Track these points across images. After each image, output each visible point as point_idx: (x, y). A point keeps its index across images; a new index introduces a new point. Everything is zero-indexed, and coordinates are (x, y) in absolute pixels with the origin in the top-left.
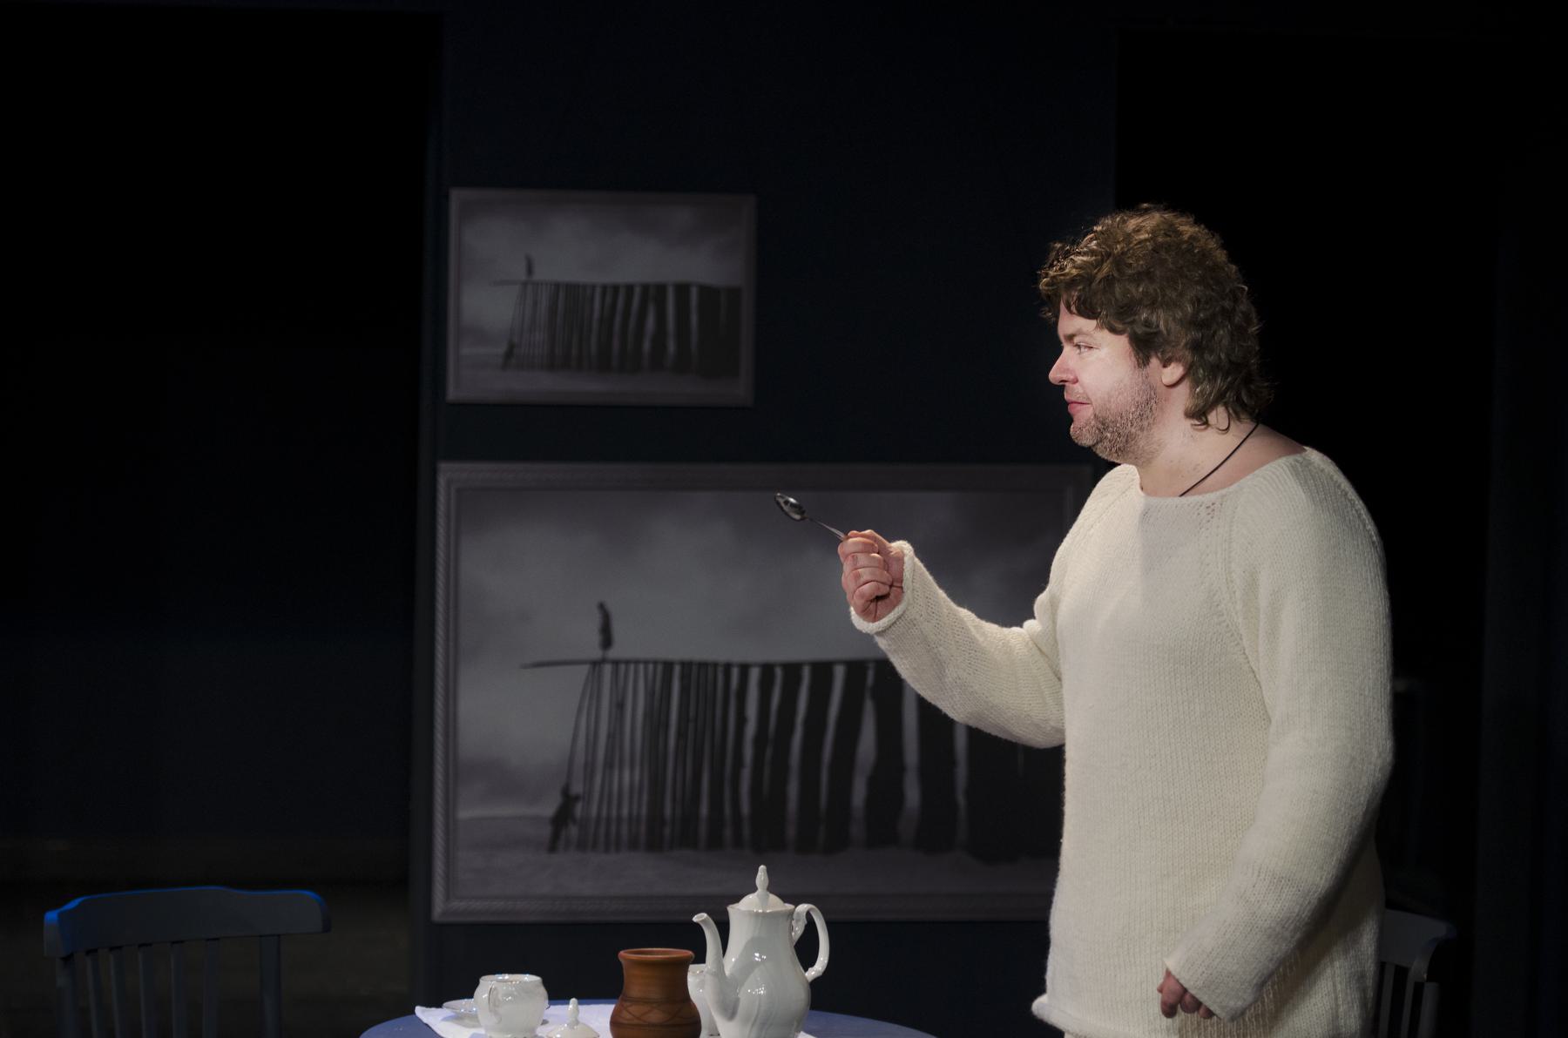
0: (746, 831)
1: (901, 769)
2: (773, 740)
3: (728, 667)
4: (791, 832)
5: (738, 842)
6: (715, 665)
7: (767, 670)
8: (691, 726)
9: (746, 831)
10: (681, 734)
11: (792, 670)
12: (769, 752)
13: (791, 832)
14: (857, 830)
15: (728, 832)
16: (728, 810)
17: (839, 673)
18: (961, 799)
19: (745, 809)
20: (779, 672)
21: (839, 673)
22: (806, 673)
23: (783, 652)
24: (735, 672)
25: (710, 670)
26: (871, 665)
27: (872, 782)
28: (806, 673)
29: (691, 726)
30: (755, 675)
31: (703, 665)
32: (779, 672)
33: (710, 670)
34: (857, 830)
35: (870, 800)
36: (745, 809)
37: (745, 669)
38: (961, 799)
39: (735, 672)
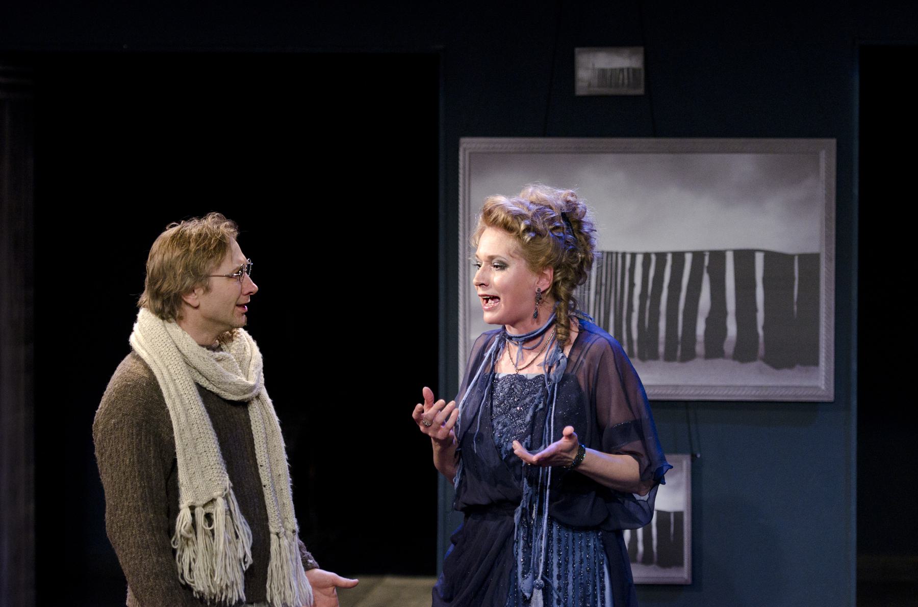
0: (636, 348)
1: (725, 313)
2: (651, 296)
3: (624, 255)
4: (661, 349)
6: (617, 253)
7: (647, 256)
8: (603, 288)
9: (636, 348)
10: (597, 293)
11: (661, 256)
13: (661, 349)
14: (700, 348)
17: (689, 258)
18: (760, 331)
19: (635, 335)
20: (653, 258)
21: (689, 258)
22: (669, 258)
24: (628, 258)
25: (614, 256)
26: (707, 254)
27: (708, 321)
28: (669, 258)
29: (603, 288)
30: (639, 259)
31: (609, 254)
32: (653, 258)
33: (614, 256)
34: (700, 348)
35: (707, 332)
36: (635, 335)
37: (634, 255)
38: (760, 331)
39: (628, 258)
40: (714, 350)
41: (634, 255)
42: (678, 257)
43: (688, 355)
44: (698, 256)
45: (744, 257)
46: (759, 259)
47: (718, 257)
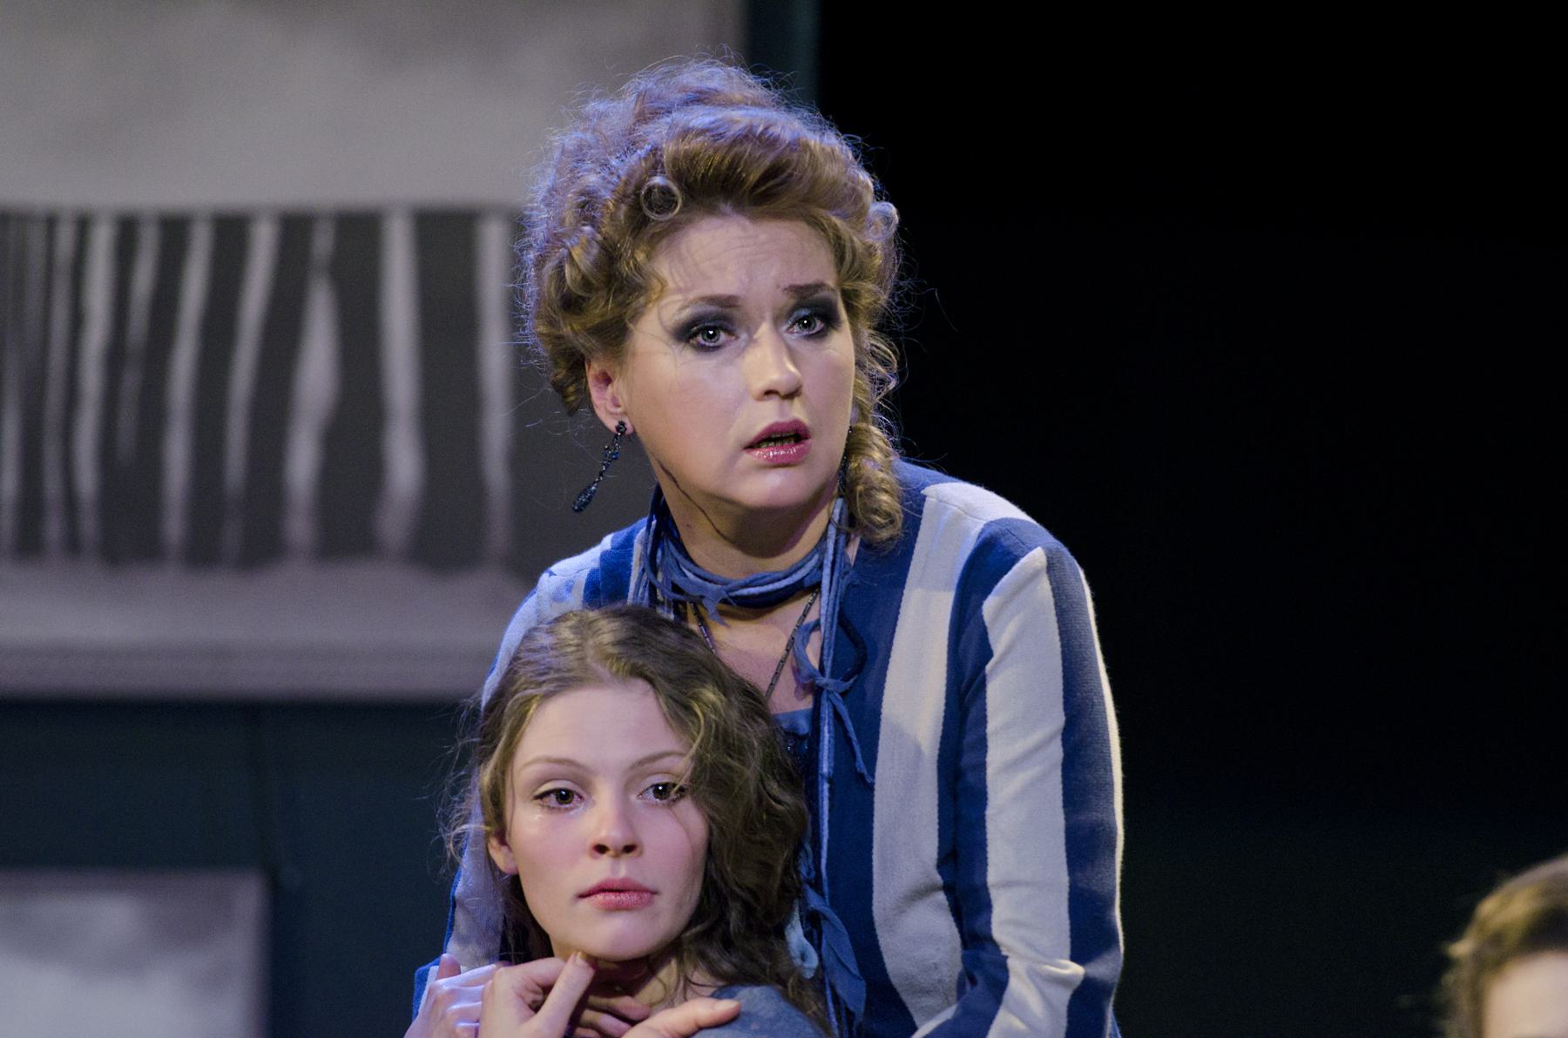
2: (139, 357)
3: (51, 222)
4: (174, 526)
5: (73, 545)
7: (127, 229)
9: (89, 525)
11: (175, 229)
12: (131, 380)
13: (174, 526)
14: (300, 526)
15: (53, 528)
16: (52, 486)
23: (155, 188)
30: (102, 240)
34: (300, 526)
40: (347, 527)
41: (84, 225)
42: (231, 232)
43: (262, 548)
44: (295, 228)
45: (446, 235)
46: (493, 241)
47: (360, 231)
